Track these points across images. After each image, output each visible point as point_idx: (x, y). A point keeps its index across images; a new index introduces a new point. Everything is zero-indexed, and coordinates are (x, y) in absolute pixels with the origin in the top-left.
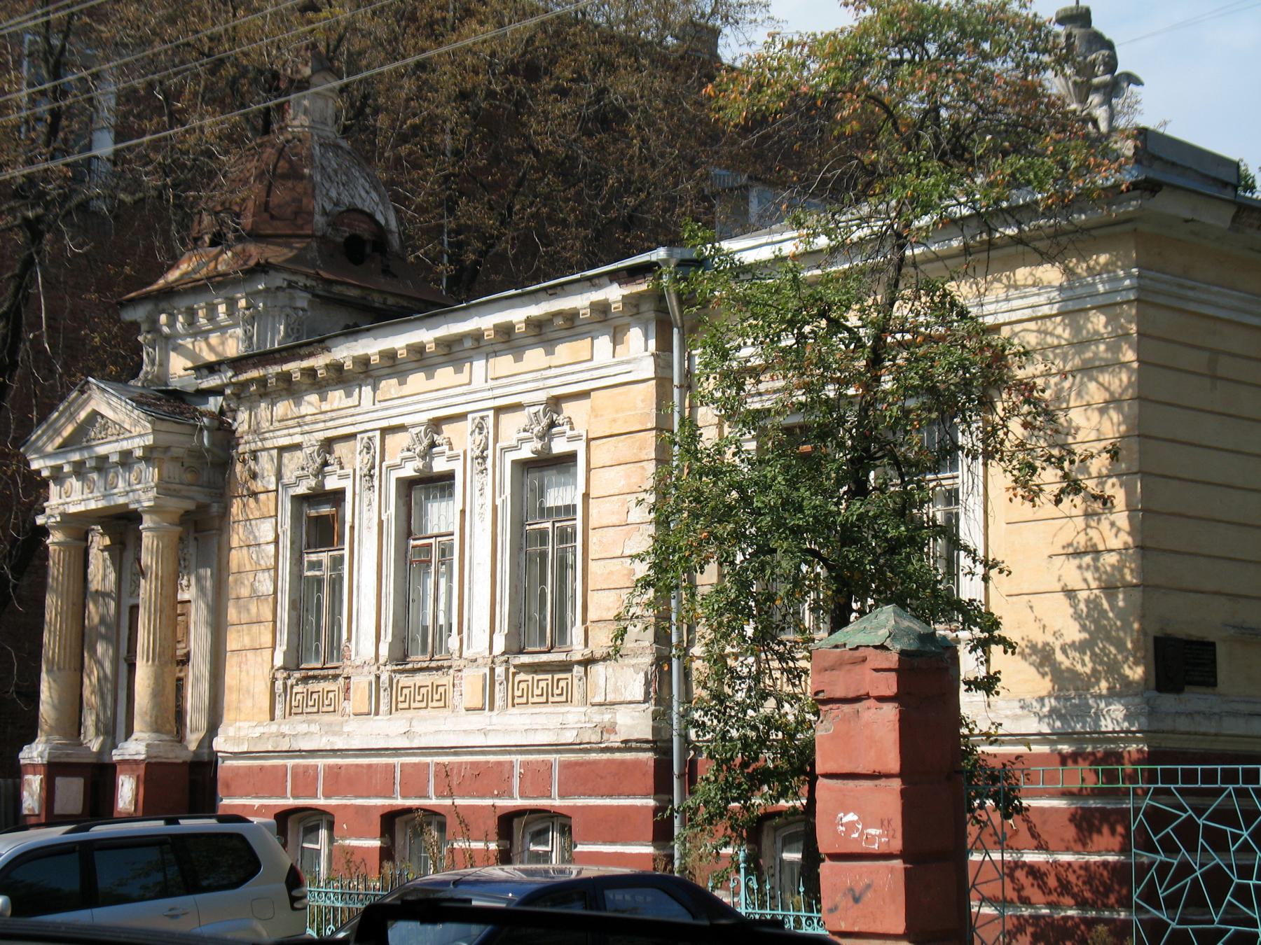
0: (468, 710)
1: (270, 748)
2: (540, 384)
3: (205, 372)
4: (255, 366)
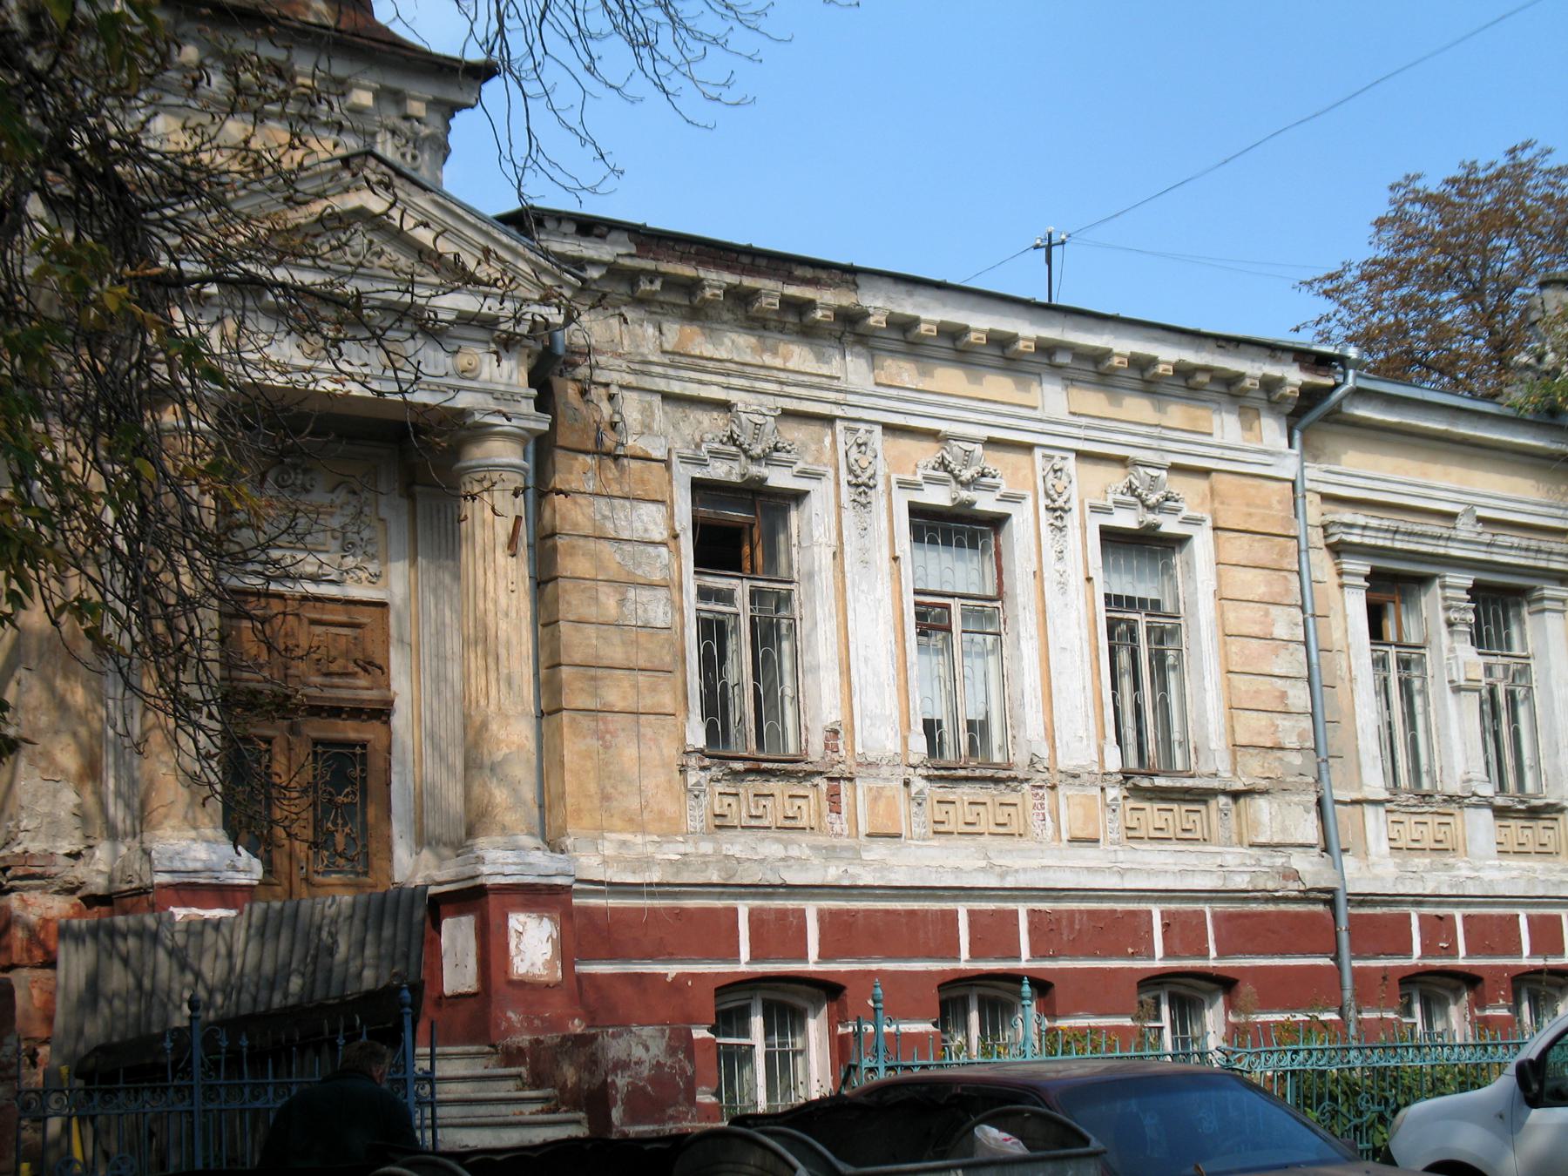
0: (1072, 840)
1: (715, 879)
2: (1155, 443)
3: (570, 228)
4: (683, 259)
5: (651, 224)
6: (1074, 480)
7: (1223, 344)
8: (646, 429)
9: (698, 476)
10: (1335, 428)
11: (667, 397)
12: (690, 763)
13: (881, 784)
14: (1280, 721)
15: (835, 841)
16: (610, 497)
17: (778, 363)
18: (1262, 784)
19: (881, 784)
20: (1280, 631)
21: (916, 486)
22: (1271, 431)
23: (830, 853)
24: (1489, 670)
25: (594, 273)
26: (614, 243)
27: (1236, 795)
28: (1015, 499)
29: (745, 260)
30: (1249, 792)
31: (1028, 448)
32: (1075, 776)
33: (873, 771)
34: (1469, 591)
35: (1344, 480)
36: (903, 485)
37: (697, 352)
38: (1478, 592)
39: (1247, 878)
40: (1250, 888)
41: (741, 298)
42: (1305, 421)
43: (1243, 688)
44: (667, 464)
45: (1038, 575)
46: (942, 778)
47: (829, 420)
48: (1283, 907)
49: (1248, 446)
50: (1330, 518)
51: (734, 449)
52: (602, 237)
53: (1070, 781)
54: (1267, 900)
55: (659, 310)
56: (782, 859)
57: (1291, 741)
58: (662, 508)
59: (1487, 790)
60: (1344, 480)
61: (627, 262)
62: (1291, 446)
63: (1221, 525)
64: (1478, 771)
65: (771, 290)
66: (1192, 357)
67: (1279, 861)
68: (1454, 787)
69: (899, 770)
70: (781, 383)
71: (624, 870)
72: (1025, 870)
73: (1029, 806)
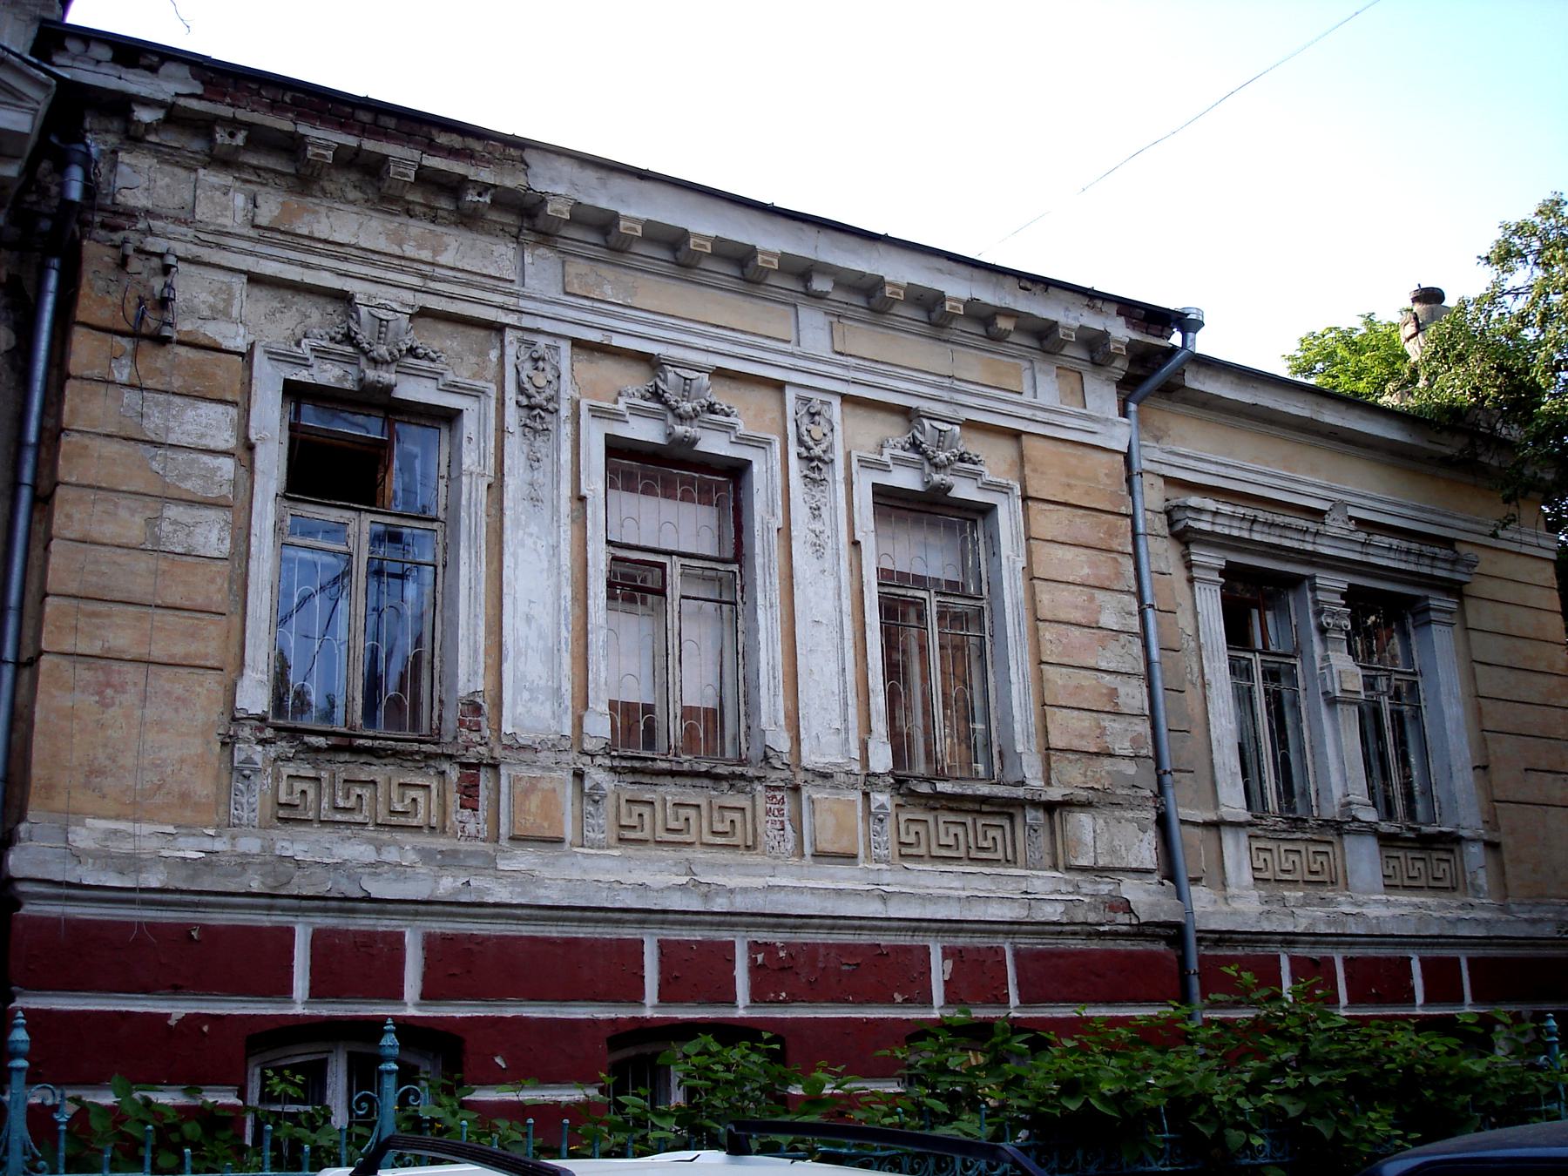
1: (256, 886)
2: (946, 395)
4: (275, 107)
5: (215, 56)
6: (838, 428)
7: (1029, 285)
8: (219, 313)
9: (294, 378)
10: (1180, 408)
11: (255, 279)
12: (241, 734)
13: (538, 773)
14: (1107, 721)
15: (464, 845)
16: (142, 389)
17: (425, 255)
18: (1083, 795)
19: (538, 773)
20: (1109, 620)
21: (616, 416)
22: (1102, 397)
23: (449, 859)
24: (1370, 684)
25: (145, 115)
26: (169, 78)
27: (1050, 807)
28: (762, 444)
29: (365, 117)
30: (1068, 804)
31: (779, 386)
32: (826, 776)
33: (527, 756)
34: (1343, 596)
35: (1191, 463)
36: (597, 413)
37: (305, 231)
38: (1352, 596)
39: (1060, 908)
40: (1065, 920)
41: (370, 169)
42: (1140, 392)
43: (1060, 682)
44: (247, 356)
45: (786, 533)
46: (634, 771)
47: (498, 328)
48: (1110, 945)
49: (1065, 408)
50: (1174, 502)
51: (350, 349)
52: (153, 70)
53: (819, 781)
54: (1089, 935)
55: (254, 178)
56: (371, 865)
57: (1123, 746)
58: (233, 412)
59: (1369, 815)
60: (1191, 463)
61: (195, 104)
62: (1124, 413)
63: (1031, 493)
64: (1359, 793)
65: (403, 156)
66: (989, 295)
67: (1105, 888)
68: (1332, 811)
69: (564, 757)
70: (424, 277)
71: (105, 868)
72: (745, 890)
73: (760, 812)
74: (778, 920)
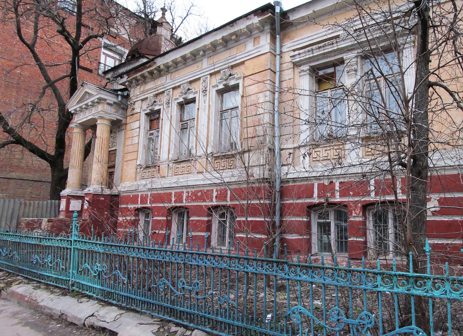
7: (231, 25)
28: (196, 93)
32: (200, 157)
74: (193, 186)
